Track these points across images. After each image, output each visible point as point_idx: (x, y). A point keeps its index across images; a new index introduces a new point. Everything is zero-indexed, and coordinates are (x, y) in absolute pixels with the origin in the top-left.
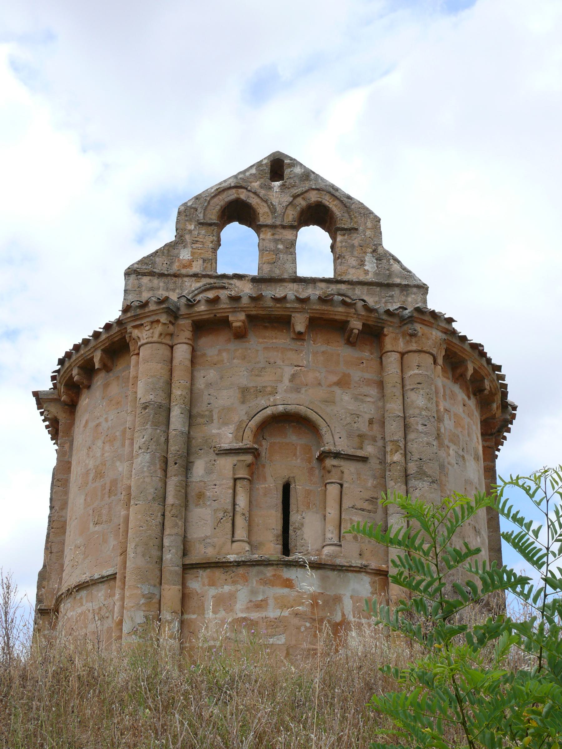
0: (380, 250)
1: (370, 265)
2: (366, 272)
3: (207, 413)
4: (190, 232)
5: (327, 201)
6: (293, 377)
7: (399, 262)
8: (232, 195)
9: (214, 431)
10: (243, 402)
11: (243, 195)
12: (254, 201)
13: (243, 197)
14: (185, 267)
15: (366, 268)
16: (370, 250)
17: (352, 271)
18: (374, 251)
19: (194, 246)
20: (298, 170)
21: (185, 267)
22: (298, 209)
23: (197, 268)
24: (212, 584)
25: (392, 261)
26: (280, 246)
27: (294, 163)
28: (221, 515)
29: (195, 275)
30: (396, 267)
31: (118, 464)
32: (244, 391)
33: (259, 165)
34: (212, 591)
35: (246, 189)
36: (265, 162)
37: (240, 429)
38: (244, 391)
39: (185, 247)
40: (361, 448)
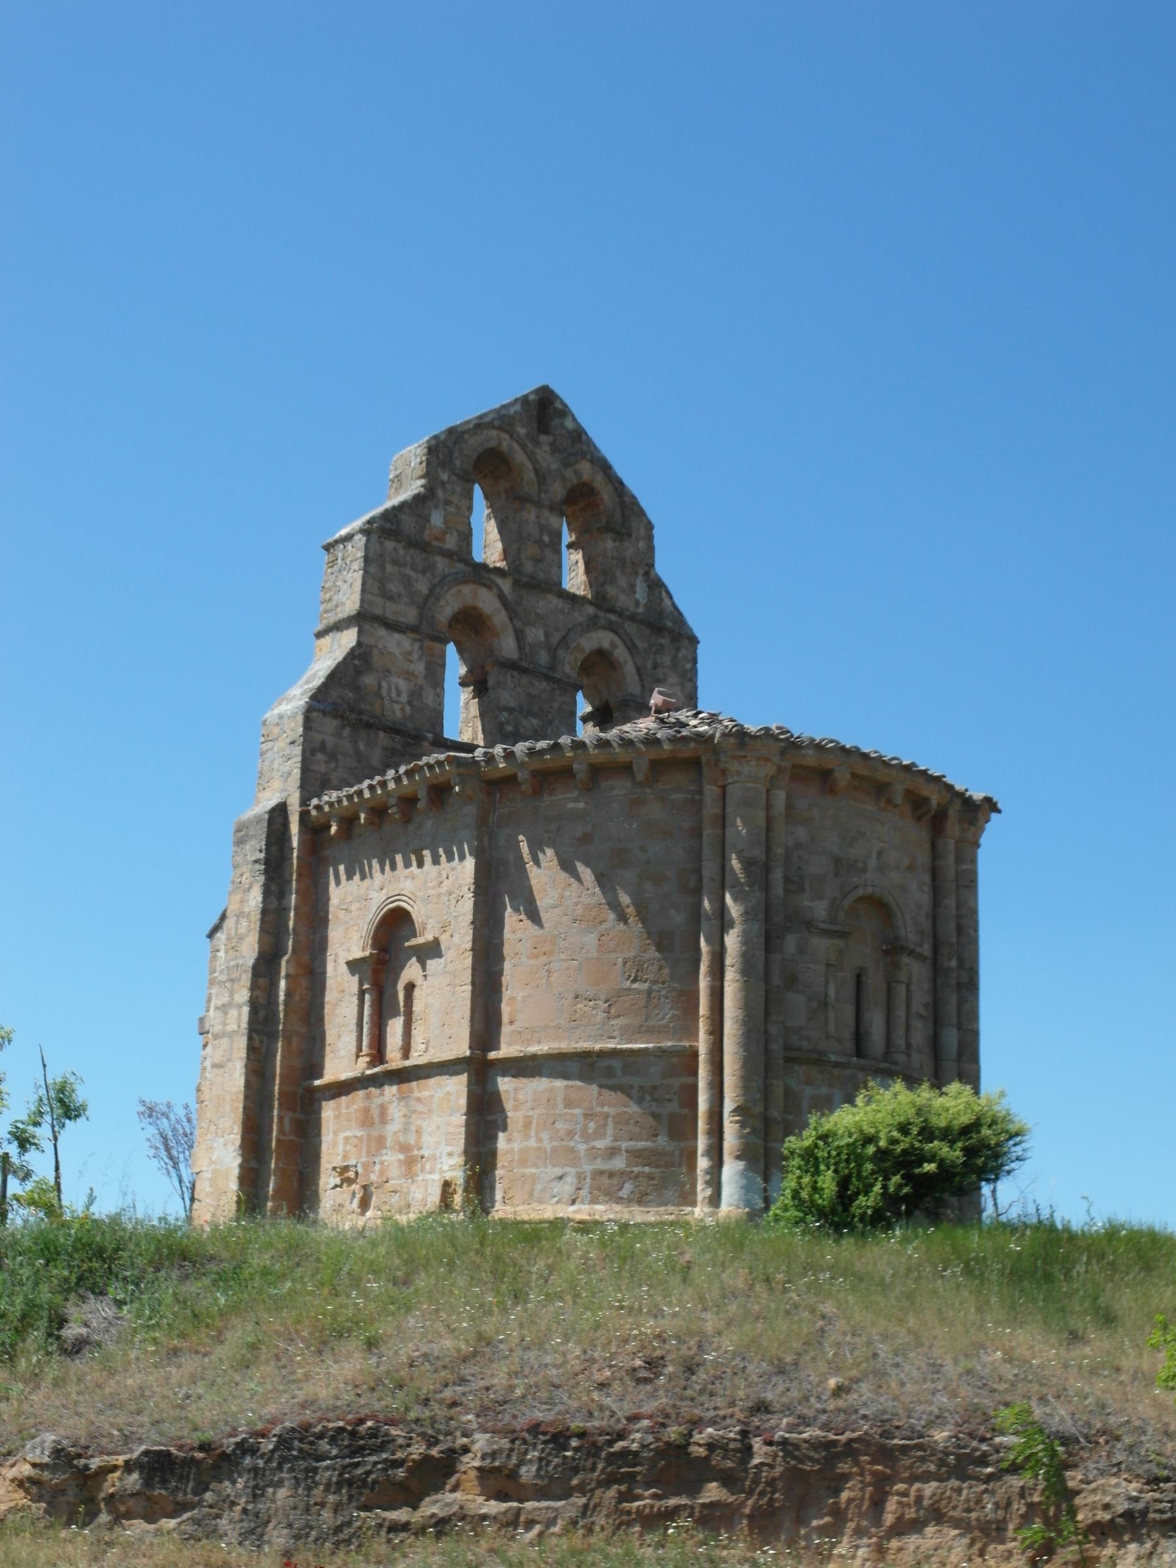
0: (652, 574)
1: (641, 594)
2: (637, 603)
3: (797, 879)
4: (443, 484)
5: (599, 482)
6: (880, 854)
7: (671, 597)
8: (493, 437)
9: (806, 903)
10: (836, 875)
11: (506, 443)
12: (520, 456)
13: (505, 446)
14: (436, 539)
15: (638, 596)
16: (641, 572)
17: (622, 597)
18: (647, 574)
19: (451, 509)
20: (569, 424)
21: (436, 539)
22: (569, 485)
23: (451, 543)
24: (809, 1082)
25: (664, 594)
26: (546, 539)
27: (565, 412)
28: (815, 1004)
29: (448, 554)
30: (667, 601)
31: (672, 912)
32: (837, 861)
33: (524, 400)
34: (809, 1091)
35: (511, 436)
36: (532, 397)
37: (834, 907)
38: (837, 861)
39: (436, 507)
40: (921, 946)
